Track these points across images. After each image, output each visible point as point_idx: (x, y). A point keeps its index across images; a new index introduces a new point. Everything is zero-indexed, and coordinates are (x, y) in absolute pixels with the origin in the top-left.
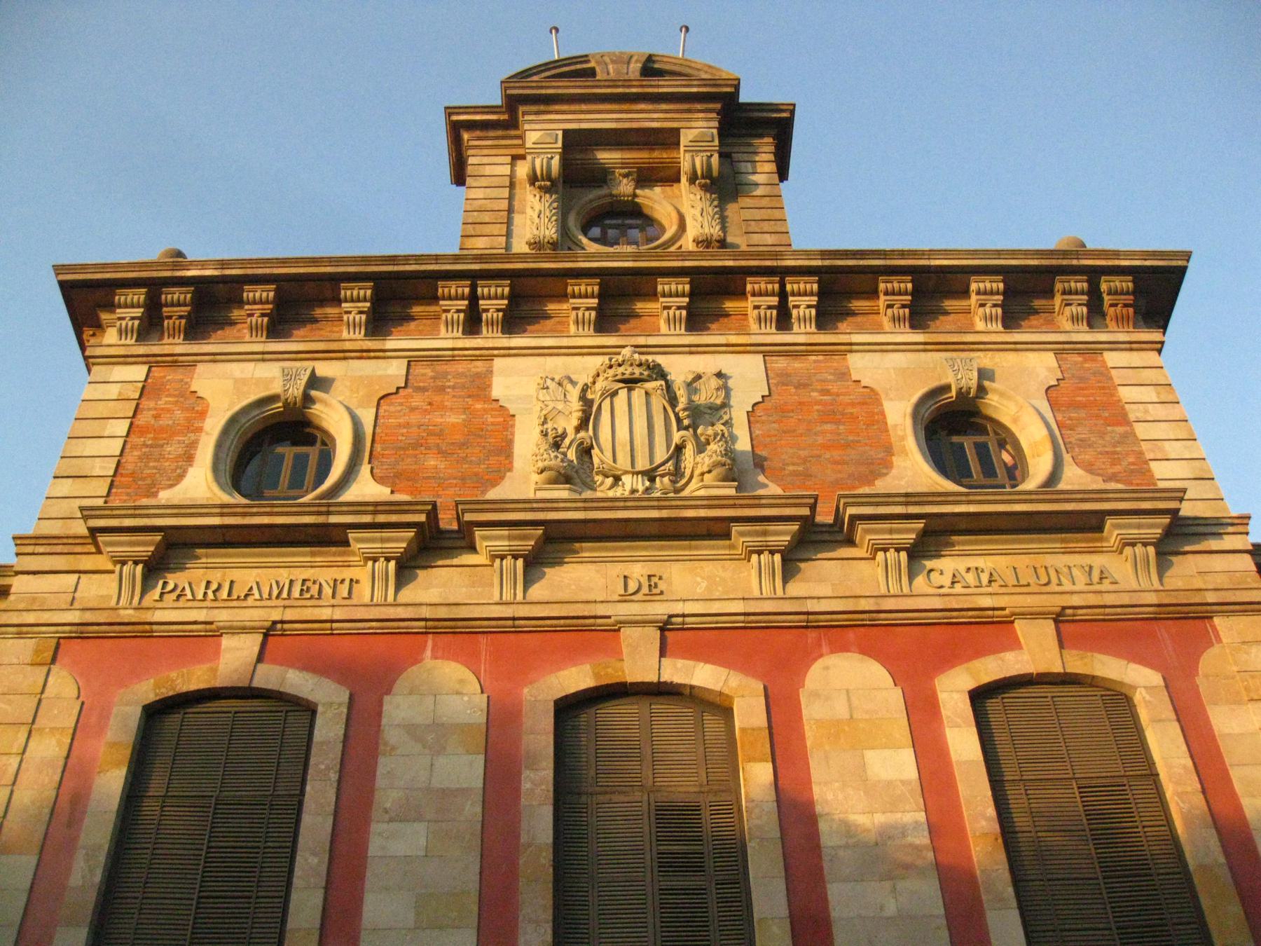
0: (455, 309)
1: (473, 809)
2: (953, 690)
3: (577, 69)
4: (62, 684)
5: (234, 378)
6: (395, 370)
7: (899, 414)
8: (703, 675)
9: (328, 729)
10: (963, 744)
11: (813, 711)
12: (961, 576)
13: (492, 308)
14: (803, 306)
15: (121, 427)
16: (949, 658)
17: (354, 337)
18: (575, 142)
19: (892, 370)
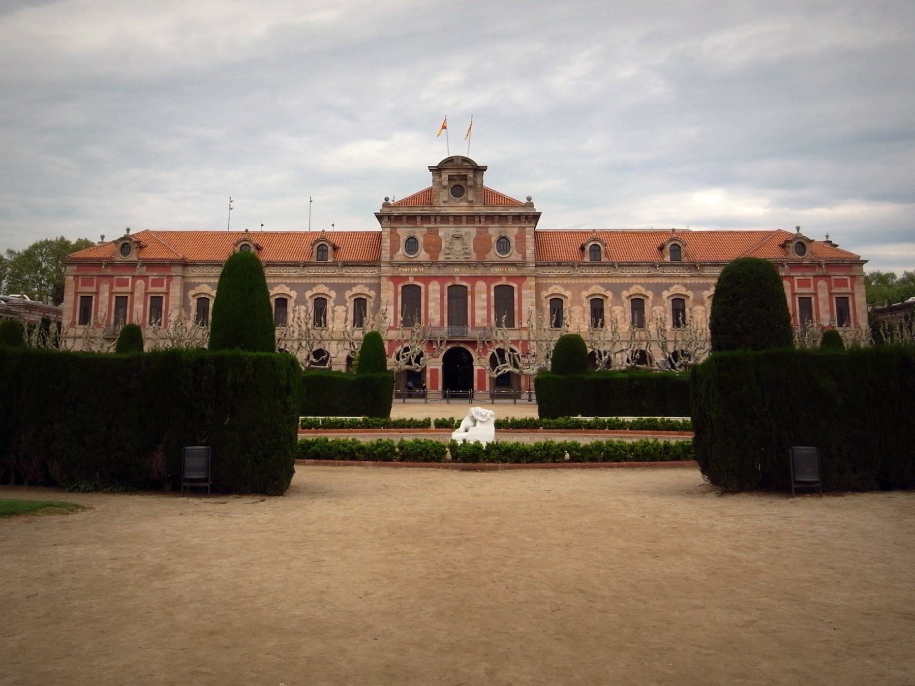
0: (433, 220)
1: (439, 301)
2: (492, 288)
3: (450, 160)
4: (391, 284)
5: (404, 232)
6: (425, 230)
7: (494, 239)
8: (464, 284)
9: (423, 290)
10: (493, 294)
11: (476, 289)
12: (497, 271)
13: (438, 219)
14: (483, 220)
15: (389, 241)
16: (492, 282)
17: (419, 224)
18: (451, 179)
19: (494, 231)
